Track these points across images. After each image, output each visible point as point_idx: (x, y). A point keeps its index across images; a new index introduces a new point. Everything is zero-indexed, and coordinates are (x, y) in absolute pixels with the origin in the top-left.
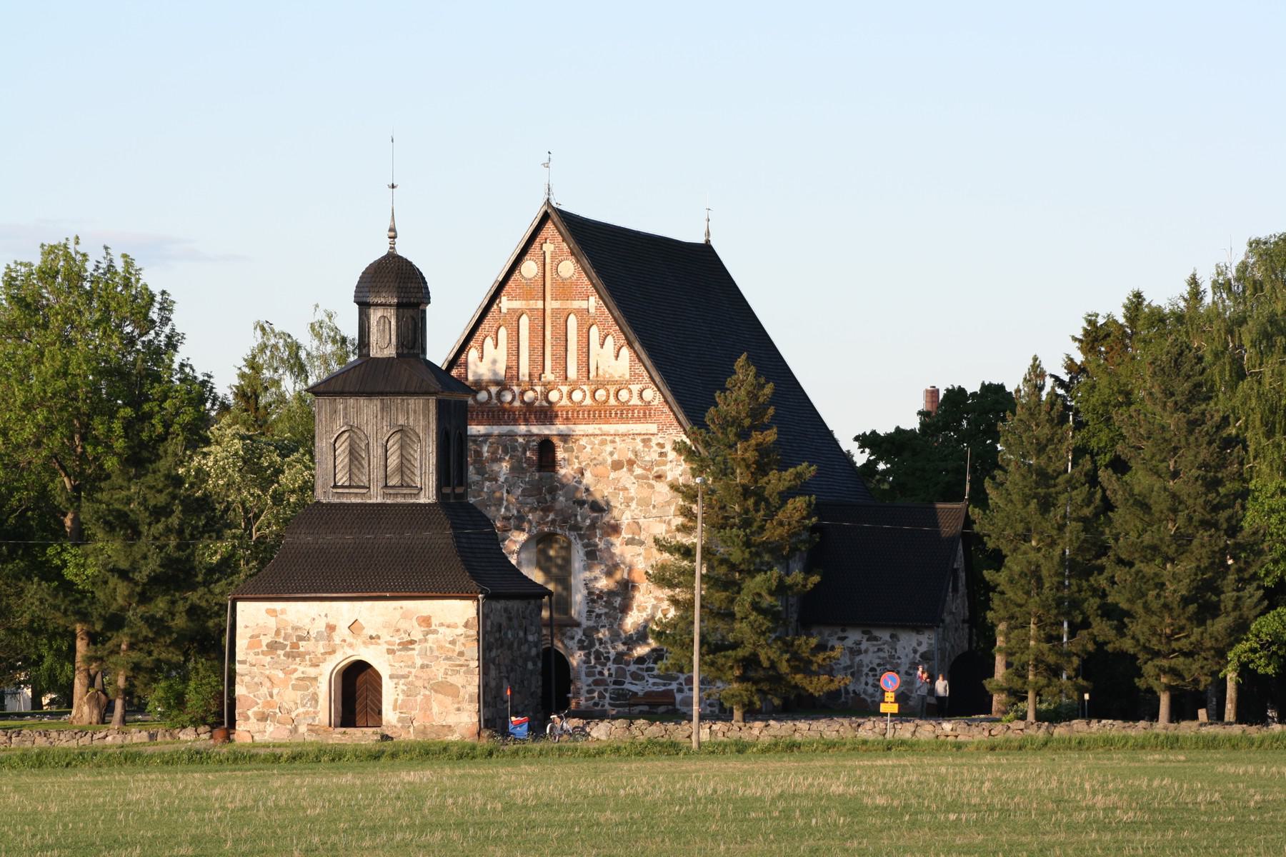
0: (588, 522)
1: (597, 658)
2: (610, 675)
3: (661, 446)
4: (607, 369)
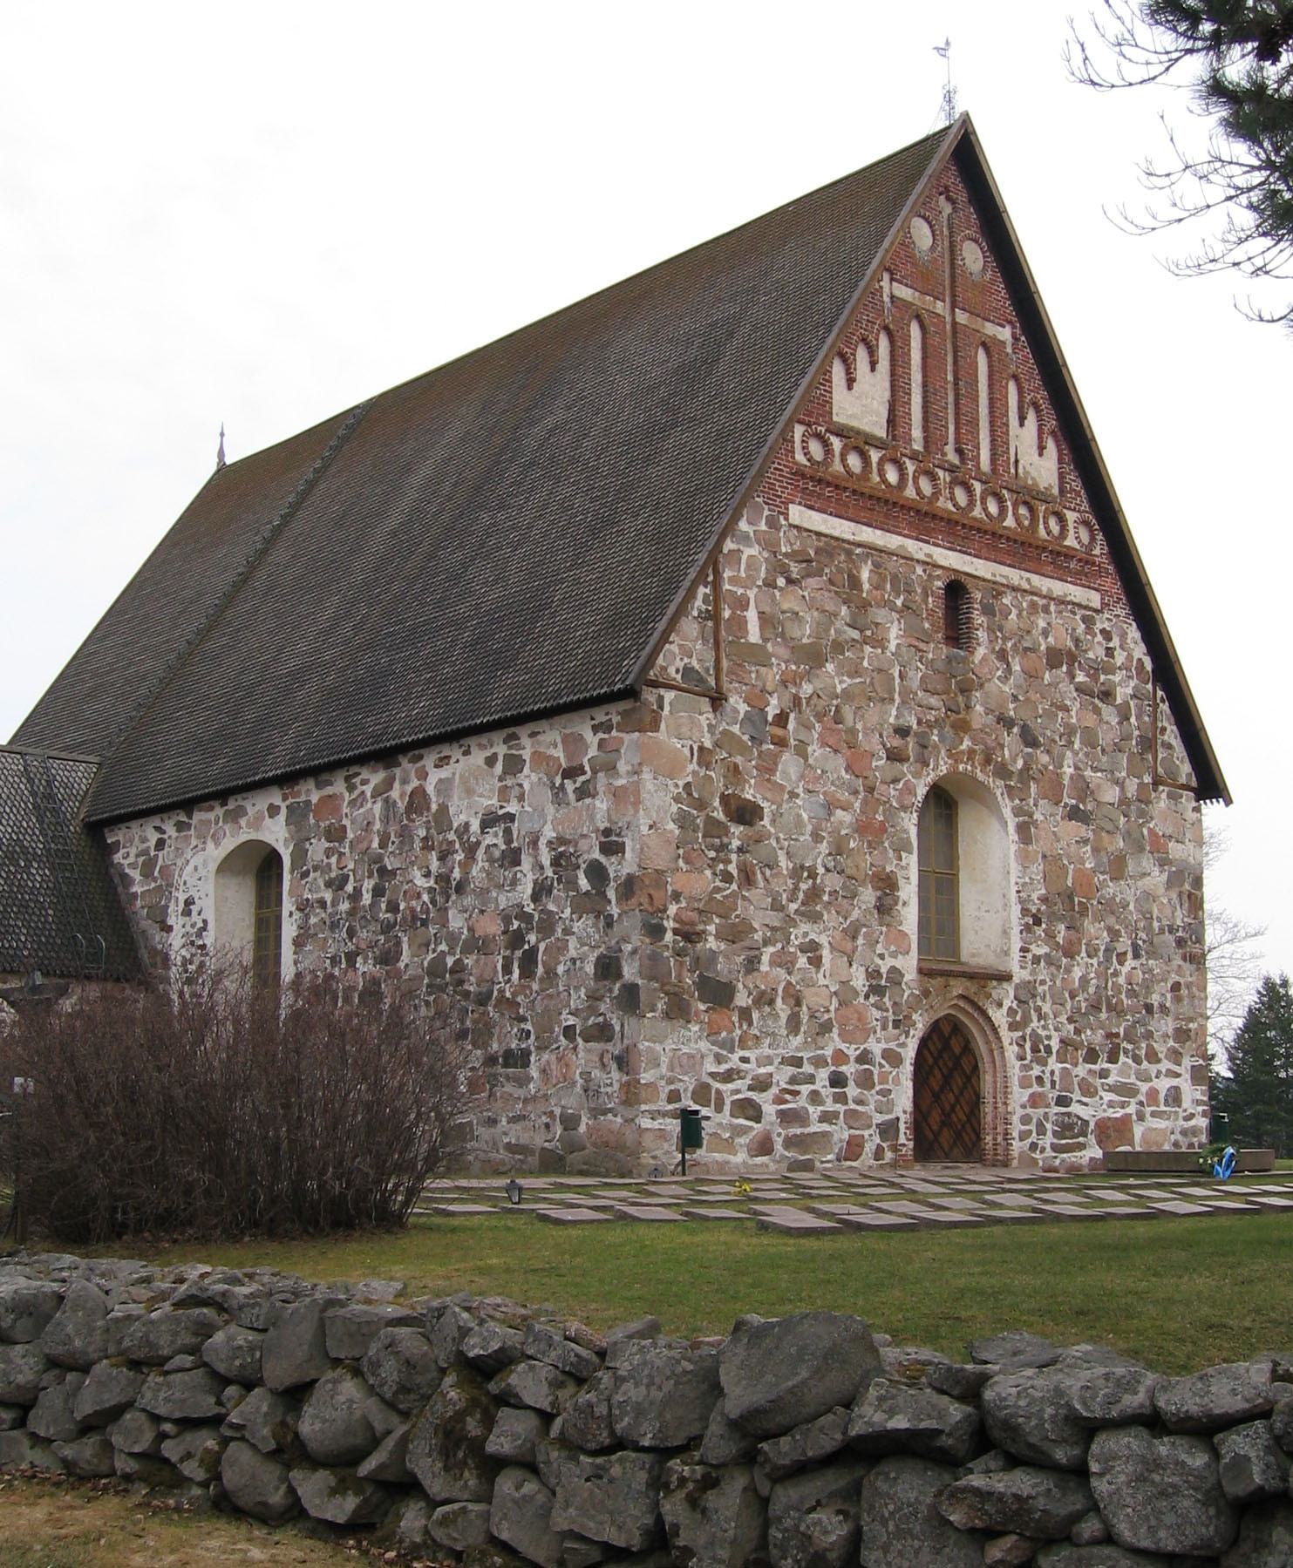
0: (1020, 763)
1: (1035, 1050)
2: (1053, 1083)
3: (1107, 635)
4: (1028, 468)
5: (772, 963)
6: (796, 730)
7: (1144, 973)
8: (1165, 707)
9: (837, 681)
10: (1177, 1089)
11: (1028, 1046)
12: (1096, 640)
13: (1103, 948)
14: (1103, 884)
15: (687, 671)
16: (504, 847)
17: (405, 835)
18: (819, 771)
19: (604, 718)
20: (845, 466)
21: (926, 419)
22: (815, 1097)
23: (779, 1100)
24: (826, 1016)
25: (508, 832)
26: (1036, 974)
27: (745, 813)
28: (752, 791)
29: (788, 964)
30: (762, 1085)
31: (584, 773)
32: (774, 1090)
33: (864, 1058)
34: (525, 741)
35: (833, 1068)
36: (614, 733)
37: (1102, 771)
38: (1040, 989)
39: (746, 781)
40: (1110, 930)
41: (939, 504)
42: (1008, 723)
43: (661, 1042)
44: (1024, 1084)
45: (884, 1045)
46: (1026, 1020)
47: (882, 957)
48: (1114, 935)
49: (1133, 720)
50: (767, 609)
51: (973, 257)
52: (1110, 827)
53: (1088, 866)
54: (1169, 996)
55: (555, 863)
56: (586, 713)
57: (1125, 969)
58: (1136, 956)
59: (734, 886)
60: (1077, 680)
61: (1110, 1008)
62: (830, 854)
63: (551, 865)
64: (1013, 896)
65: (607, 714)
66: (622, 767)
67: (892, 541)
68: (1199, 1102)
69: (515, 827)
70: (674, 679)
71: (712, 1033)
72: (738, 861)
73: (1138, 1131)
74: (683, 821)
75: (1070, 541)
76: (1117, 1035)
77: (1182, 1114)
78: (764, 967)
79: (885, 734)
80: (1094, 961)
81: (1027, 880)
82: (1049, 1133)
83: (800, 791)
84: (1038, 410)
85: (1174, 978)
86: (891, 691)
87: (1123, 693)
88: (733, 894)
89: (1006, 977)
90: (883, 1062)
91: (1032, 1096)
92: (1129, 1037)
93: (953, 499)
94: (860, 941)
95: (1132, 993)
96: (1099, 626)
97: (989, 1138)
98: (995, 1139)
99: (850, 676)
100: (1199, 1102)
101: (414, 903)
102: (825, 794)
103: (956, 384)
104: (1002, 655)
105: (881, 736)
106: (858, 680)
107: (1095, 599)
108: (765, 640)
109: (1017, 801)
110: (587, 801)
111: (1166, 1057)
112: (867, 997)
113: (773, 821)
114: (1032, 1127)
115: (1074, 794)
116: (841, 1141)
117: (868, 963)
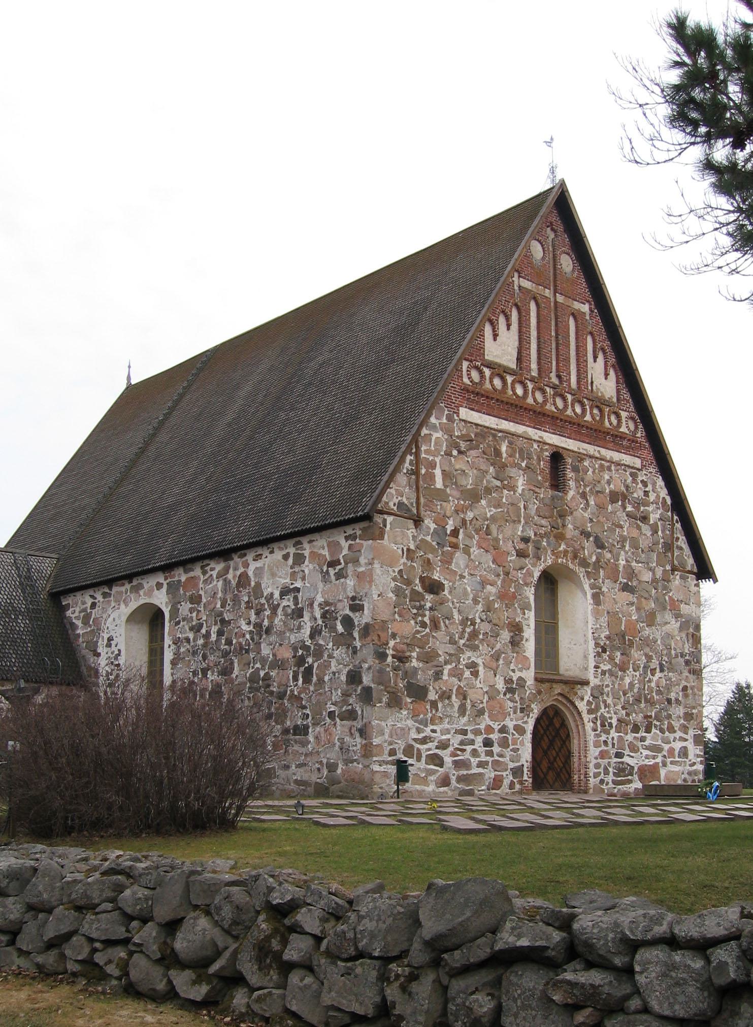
0: (594, 558)
1: (603, 725)
2: (613, 744)
3: (645, 484)
4: (599, 386)
5: (450, 675)
6: (463, 539)
7: (666, 680)
8: (678, 526)
9: (487, 511)
10: (685, 748)
11: (599, 723)
12: (638, 486)
13: (642, 666)
14: (642, 628)
15: (400, 505)
16: (293, 607)
17: (236, 600)
18: (477, 563)
19: (352, 532)
20: (492, 385)
21: (539, 358)
22: (475, 753)
23: (453, 755)
24: (481, 706)
25: (296, 598)
26: (603, 681)
27: (434, 588)
28: (438, 575)
29: (459, 676)
30: (443, 745)
31: (340, 564)
32: (451, 749)
33: (503, 730)
34: (306, 545)
35: (485, 736)
36: (358, 541)
37: (642, 563)
38: (606, 690)
39: (435, 569)
40: (646, 655)
41: (547, 407)
42: (587, 535)
43: (385, 721)
44: (597, 745)
45: (515, 723)
46: (598, 708)
47: (513, 671)
48: (649, 658)
49: (660, 533)
50: (447, 469)
51: (567, 263)
52: (646, 595)
53: (634, 618)
54: (681, 694)
55: (324, 616)
56: (341, 529)
57: (655, 678)
58: (662, 671)
59: (428, 630)
60: (627, 510)
61: (647, 701)
62: (483, 611)
63: (321, 617)
64: (590, 636)
65: (353, 530)
66: (363, 560)
67: (520, 429)
68: (698, 756)
69: (300, 595)
70: (393, 509)
71: (415, 715)
72: (430, 615)
73: (663, 772)
74: (398, 592)
75: (623, 429)
76: (651, 717)
77: (688, 763)
78: (445, 677)
79: (515, 541)
80: (637, 674)
81: (598, 626)
82: (611, 774)
83: (466, 574)
84: (604, 352)
85: (684, 683)
86: (519, 516)
87: (654, 517)
88: (427, 634)
89: (586, 683)
90: (514, 732)
91: (601, 752)
92: (657, 718)
93: (555, 404)
94: (501, 662)
95: (659, 692)
96: (640, 478)
97: (576, 777)
98: (579, 777)
99: (495, 507)
100: (698, 756)
101: (241, 640)
102: (480, 576)
103: (557, 337)
104: (584, 495)
105: (513, 542)
106: (499, 510)
107: (638, 463)
108: (446, 486)
109: (592, 581)
110: (342, 580)
111: (679, 730)
112: (505, 694)
113: (450, 592)
114: (601, 770)
115: (625, 576)
116: (490, 778)
117: (506, 675)
